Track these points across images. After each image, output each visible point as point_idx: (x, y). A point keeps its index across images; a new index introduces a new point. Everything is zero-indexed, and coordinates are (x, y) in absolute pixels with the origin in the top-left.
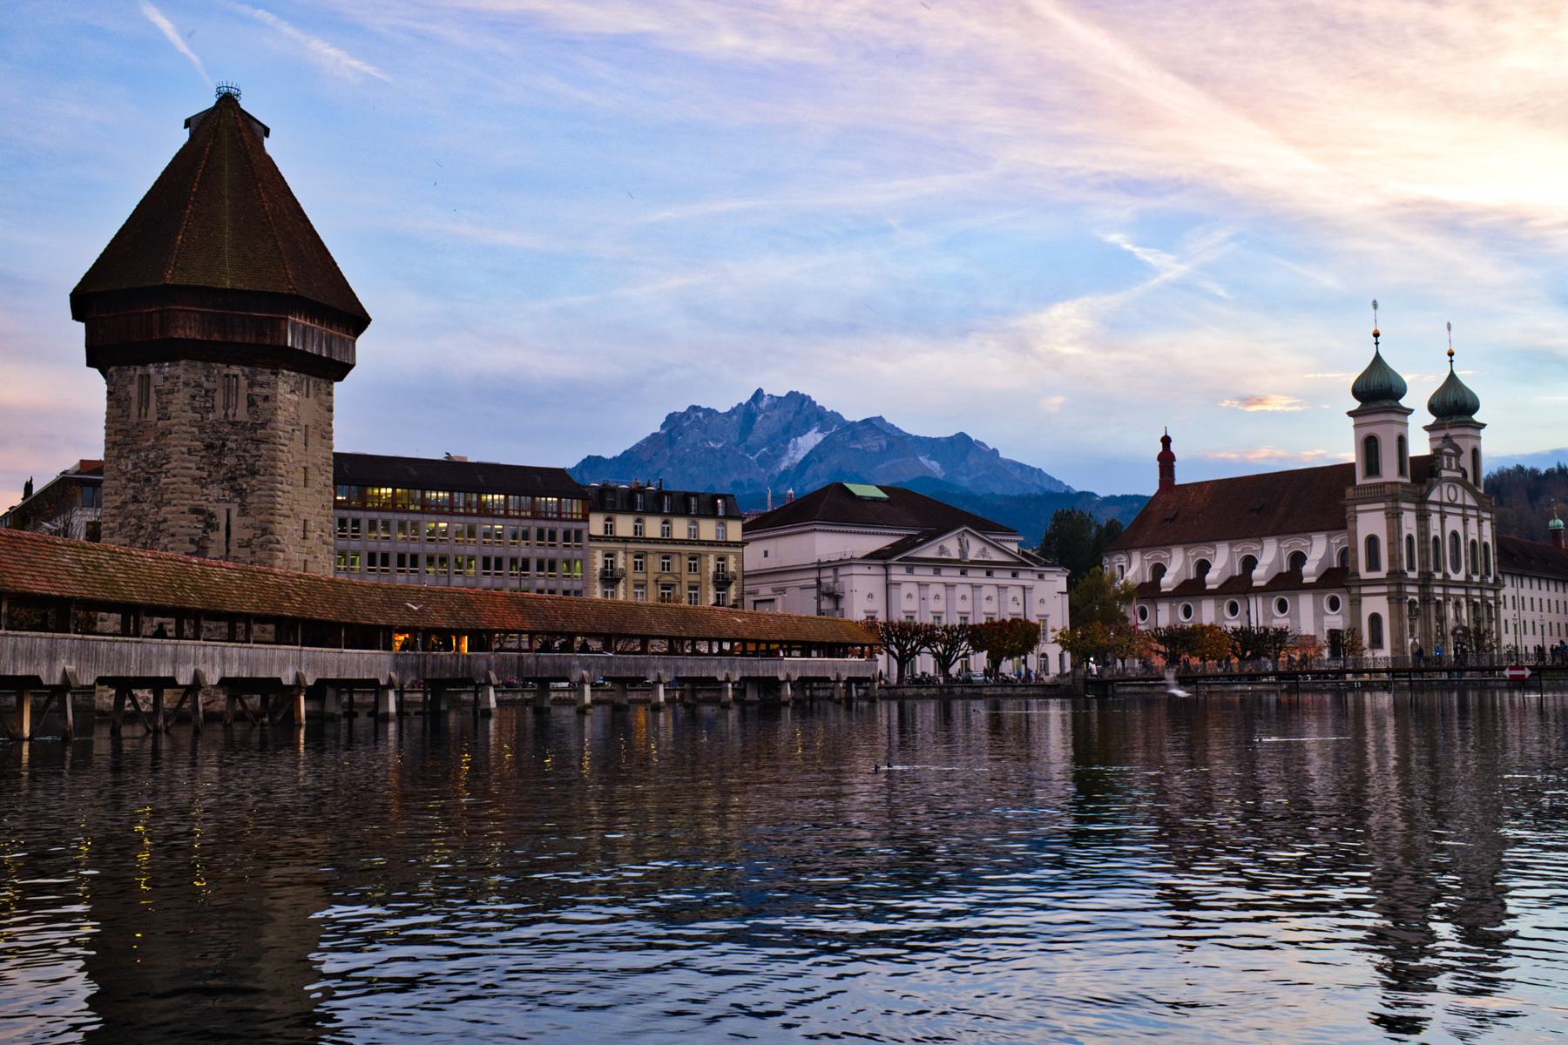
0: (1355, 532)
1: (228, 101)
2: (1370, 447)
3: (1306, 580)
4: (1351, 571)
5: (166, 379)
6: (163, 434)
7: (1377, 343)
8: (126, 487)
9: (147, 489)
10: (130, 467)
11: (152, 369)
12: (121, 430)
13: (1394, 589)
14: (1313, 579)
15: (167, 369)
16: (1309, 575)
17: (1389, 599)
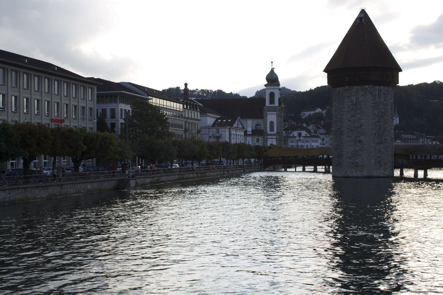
0: (266, 120)
1: (363, 12)
2: (272, 95)
3: (248, 133)
4: (264, 131)
5: (386, 91)
6: (385, 105)
7: (272, 65)
8: (376, 118)
9: (382, 119)
10: (377, 113)
11: (382, 87)
12: (374, 103)
13: (278, 137)
14: (251, 133)
15: (386, 88)
16: (249, 132)
17: (276, 140)
